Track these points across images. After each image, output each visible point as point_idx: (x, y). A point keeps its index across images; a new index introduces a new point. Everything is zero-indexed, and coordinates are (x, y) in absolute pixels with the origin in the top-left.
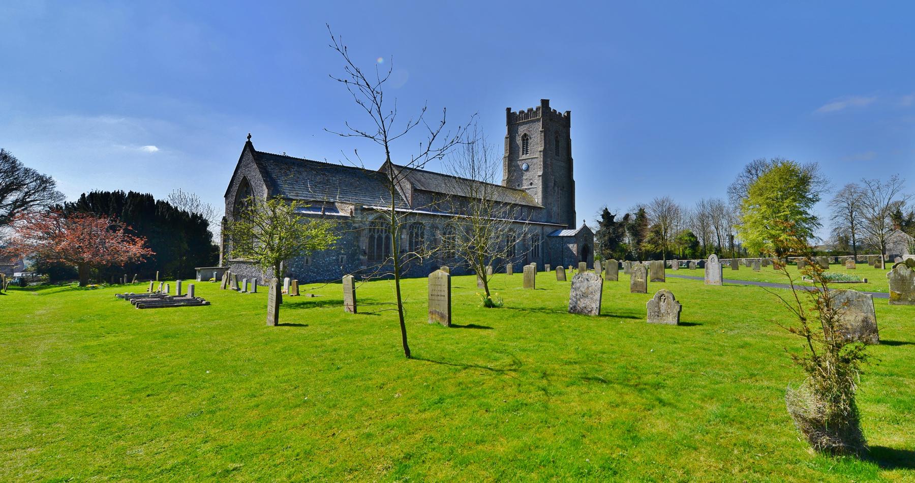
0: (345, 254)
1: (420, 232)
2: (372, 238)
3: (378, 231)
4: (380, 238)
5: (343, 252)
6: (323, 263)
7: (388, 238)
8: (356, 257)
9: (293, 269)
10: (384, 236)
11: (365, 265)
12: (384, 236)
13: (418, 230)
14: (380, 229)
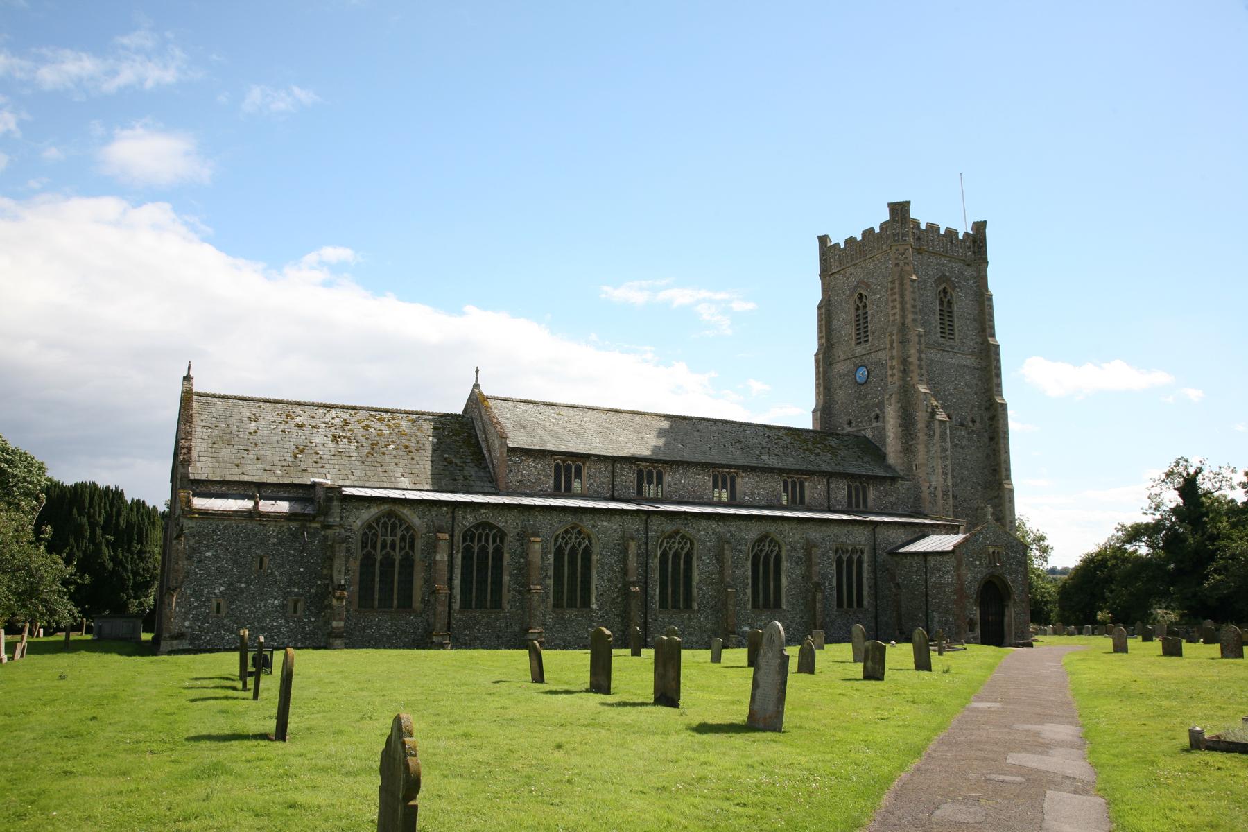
0: (302, 595)
1: (491, 550)
2: (367, 563)
3: (384, 547)
4: (388, 562)
5: (296, 590)
6: (251, 612)
7: (408, 563)
8: (326, 602)
9: (187, 624)
10: (397, 556)
11: (340, 620)
12: (397, 556)
13: (487, 541)
14: (389, 542)
